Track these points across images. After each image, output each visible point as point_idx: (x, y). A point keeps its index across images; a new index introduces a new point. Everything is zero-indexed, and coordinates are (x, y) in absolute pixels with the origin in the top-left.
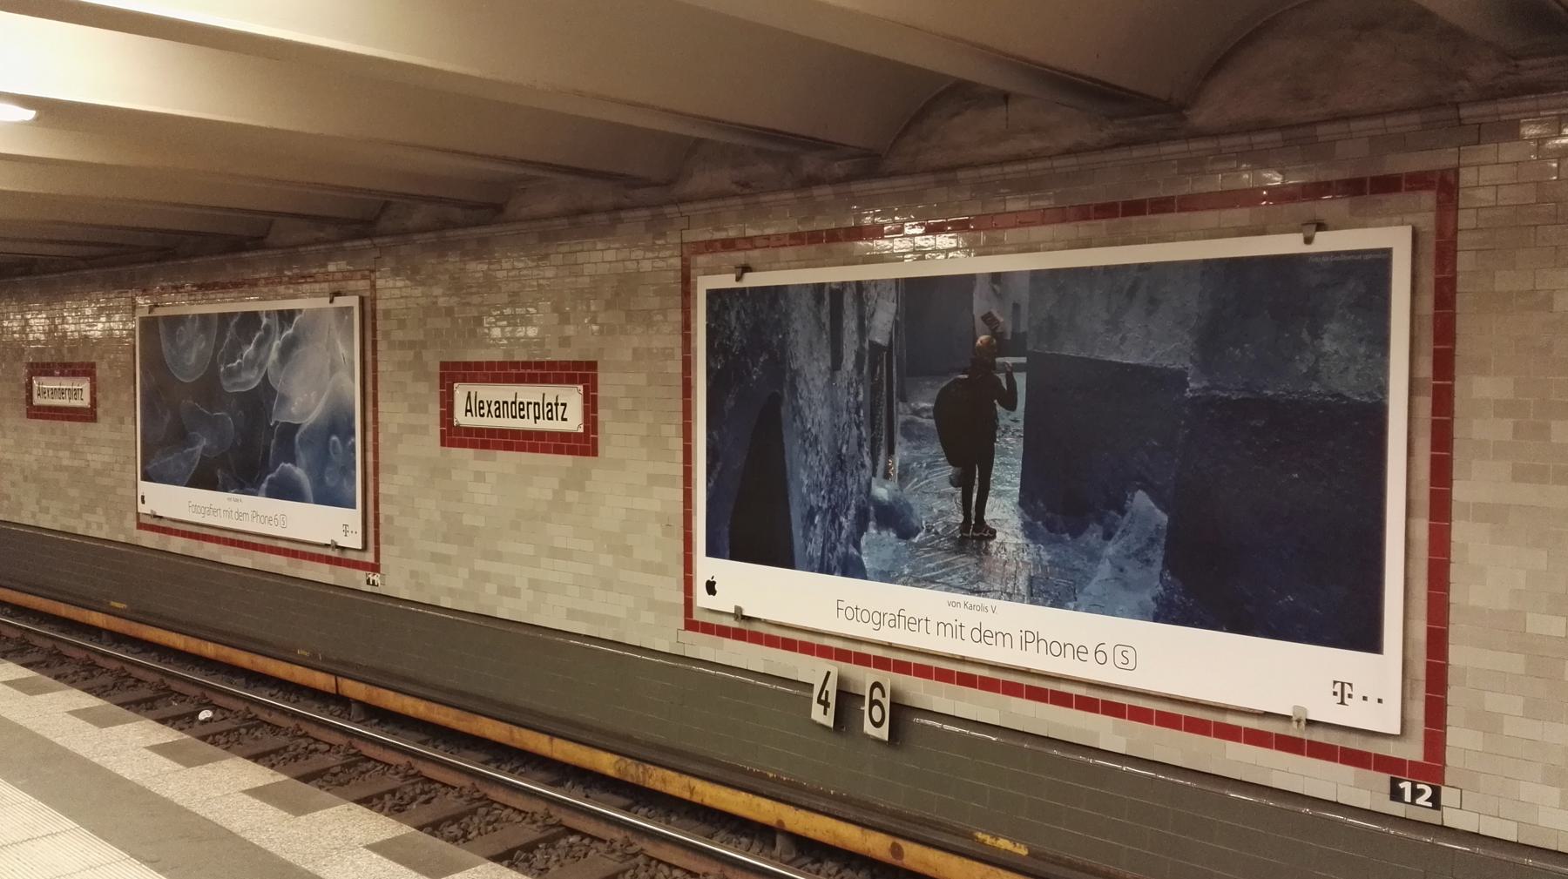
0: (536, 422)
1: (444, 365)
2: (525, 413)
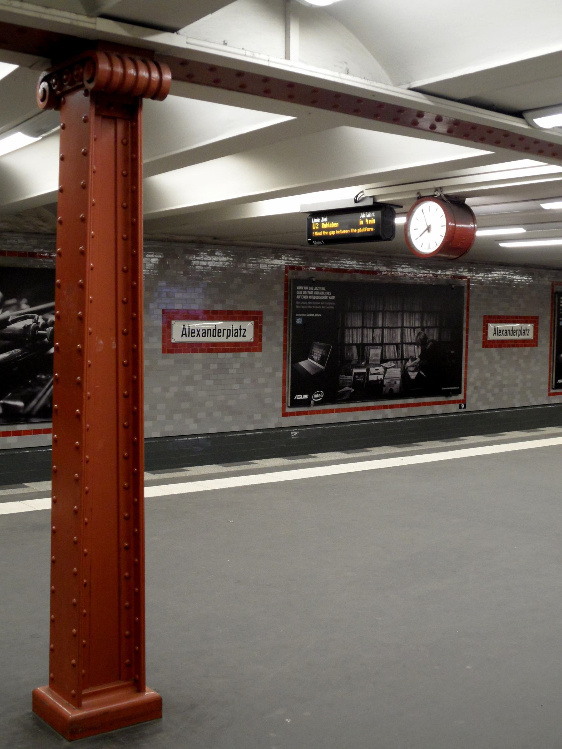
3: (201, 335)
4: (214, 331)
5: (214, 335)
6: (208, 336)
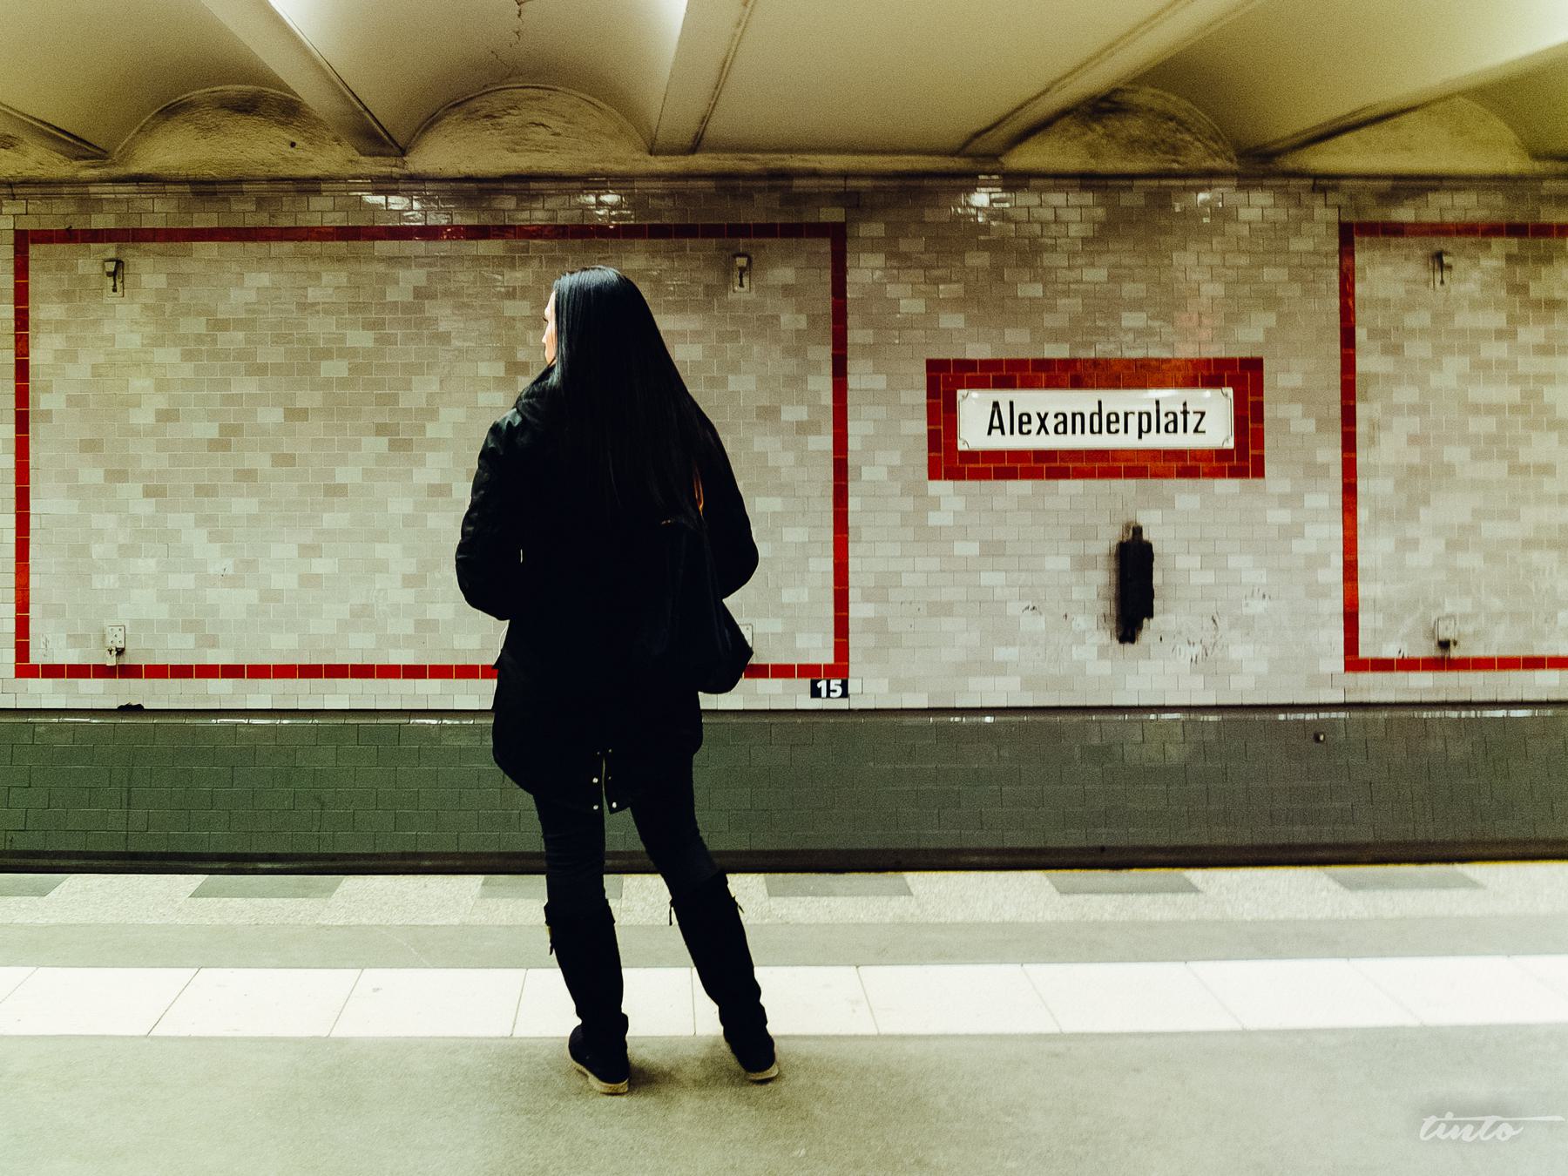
0: (1140, 437)
1: (934, 367)
3: (1051, 429)
4: (1096, 418)
6: (1074, 432)
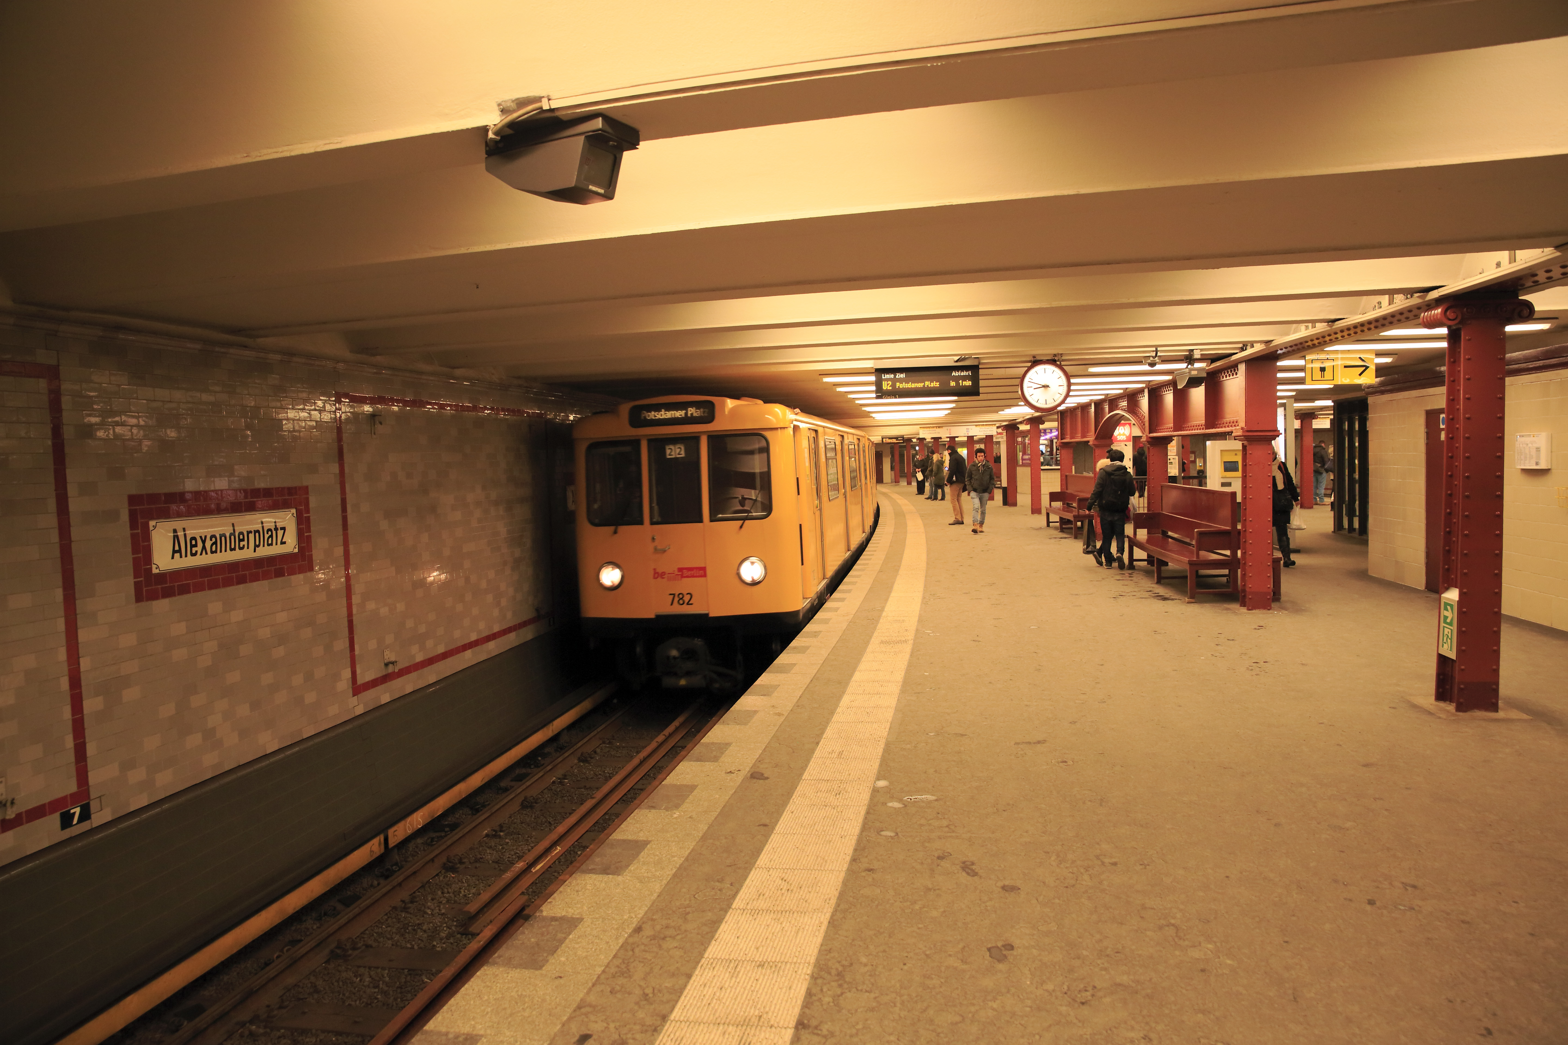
0: (255, 551)
2: (245, 543)
5: (233, 547)
6: (221, 552)
